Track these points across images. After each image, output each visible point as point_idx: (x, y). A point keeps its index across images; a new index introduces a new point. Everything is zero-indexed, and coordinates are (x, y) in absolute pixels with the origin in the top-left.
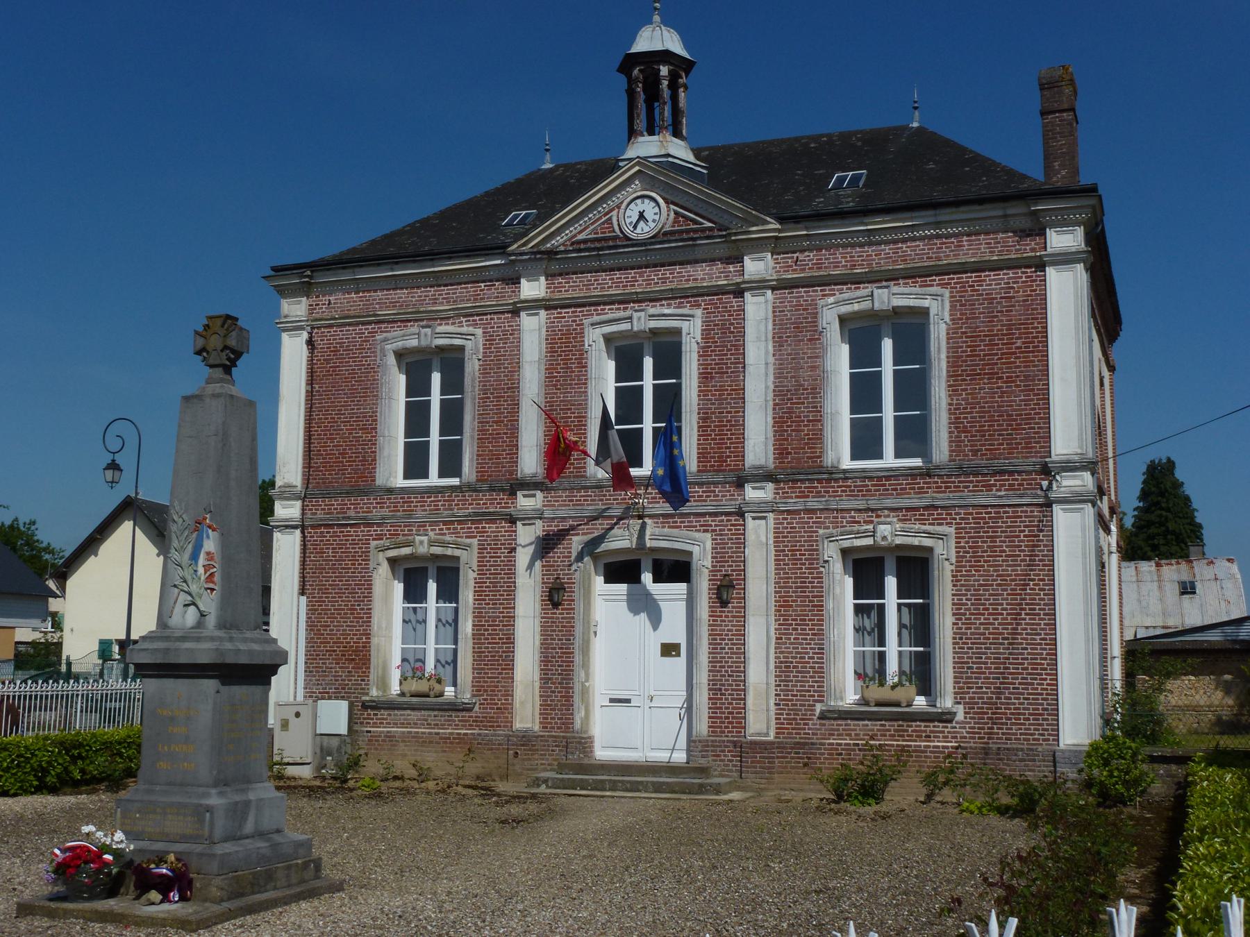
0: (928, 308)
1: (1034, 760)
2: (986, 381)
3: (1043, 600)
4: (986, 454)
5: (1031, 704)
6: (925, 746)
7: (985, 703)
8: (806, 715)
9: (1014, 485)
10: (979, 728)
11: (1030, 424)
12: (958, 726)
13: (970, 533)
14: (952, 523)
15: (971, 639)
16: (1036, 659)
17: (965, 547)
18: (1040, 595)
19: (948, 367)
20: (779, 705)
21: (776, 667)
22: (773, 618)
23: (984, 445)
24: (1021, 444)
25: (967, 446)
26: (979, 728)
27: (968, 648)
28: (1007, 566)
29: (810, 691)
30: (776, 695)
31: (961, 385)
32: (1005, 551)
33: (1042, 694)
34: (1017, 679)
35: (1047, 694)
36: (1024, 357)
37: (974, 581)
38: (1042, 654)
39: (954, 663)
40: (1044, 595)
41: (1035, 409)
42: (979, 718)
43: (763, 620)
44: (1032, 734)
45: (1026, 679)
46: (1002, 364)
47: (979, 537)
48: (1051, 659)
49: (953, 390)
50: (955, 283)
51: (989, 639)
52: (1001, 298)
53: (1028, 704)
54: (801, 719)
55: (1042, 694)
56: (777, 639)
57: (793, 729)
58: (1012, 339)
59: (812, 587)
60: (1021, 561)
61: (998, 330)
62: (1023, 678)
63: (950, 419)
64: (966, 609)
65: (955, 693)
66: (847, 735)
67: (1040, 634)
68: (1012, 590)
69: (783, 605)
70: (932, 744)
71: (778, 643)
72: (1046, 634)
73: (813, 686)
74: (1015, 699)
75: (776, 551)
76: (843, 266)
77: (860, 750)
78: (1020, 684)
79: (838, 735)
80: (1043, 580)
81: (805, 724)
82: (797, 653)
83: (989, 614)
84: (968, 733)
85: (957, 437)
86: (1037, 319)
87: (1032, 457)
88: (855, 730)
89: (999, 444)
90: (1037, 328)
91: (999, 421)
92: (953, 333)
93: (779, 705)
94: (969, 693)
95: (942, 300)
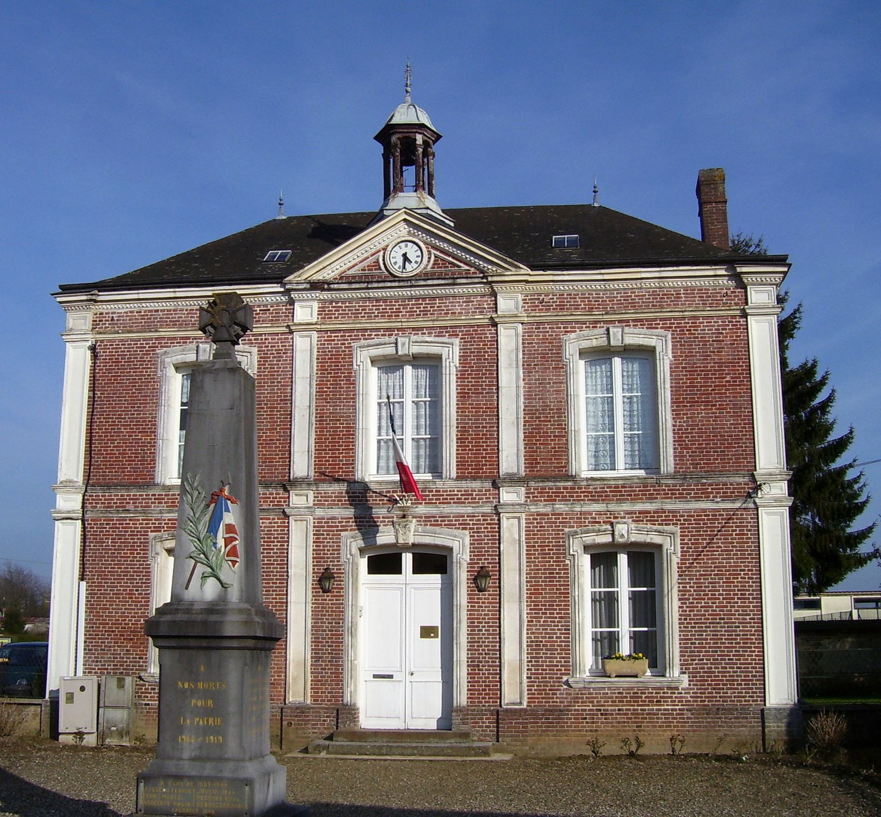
0: (654, 347)
1: (747, 718)
2: (702, 407)
3: (752, 586)
4: (704, 467)
5: (742, 672)
6: (657, 710)
7: (705, 672)
8: (554, 686)
9: (727, 493)
10: (701, 693)
11: (739, 443)
12: (683, 692)
13: (693, 532)
14: (677, 524)
15: (694, 619)
16: (747, 635)
17: (688, 544)
18: (749, 582)
19: (671, 395)
20: (530, 678)
21: (528, 646)
22: (525, 604)
23: (703, 460)
24: (731, 459)
25: (688, 460)
26: (701, 693)
27: (691, 627)
28: (723, 559)
29: (558, 666)
30: (528, 670)
31: (682, 410)
32: (720, 547)
33: (752, 664)
34: (732, 651)
35: (755, 664)
36: (733, 389)
37: (696, 571)
38: (751, 631)
39: (680, 639)
40: (753, 582)
41: (742, 431)
42: (701, 685)
43: (516, 606)
44: (743, 697)
45: (739, 651)
46: (715, 394)
47: (700, 535)
48: (758, 635)
49: (676, 415)
50: (675, 327)
51: (708, 619)
52: (713, 341)
53: (740, 672)
54: (549, 690)
55: (752, 664)
56: (528, 621)
57: (543, 698)
58: (723, 374)
59: (559, 577)
60: (734, 555)
61: (711, 367)
62: (736, 651)
63: (674, 437)
64: (690, 595)
65: (681, 665)
66: (590, 702)
67: (750, 615)
68: (726, 578)
69: (534, 592)
70: (663, 708)
71: (530, 626)
72: (754, 615)
73: (561, 662)
74: (730, 668)
75: (527, 546)
76: (582, 308)
77: (602, 714)
78: (734, 655)
79: (582, 702)
80: (752, 570)
81: (553, 694)
82: (546, 633)
83: (708, 599)
84: (691, 697)
85: (680, 452)
86: (742, 359)
87: (741, 470)
88: (597, 698)
89: (714, 460)
90: (743, 366)
91: (714, 440)
92: (675, 368)
93: (530, 678)
94: (692, 664)
95: (666, 341)
